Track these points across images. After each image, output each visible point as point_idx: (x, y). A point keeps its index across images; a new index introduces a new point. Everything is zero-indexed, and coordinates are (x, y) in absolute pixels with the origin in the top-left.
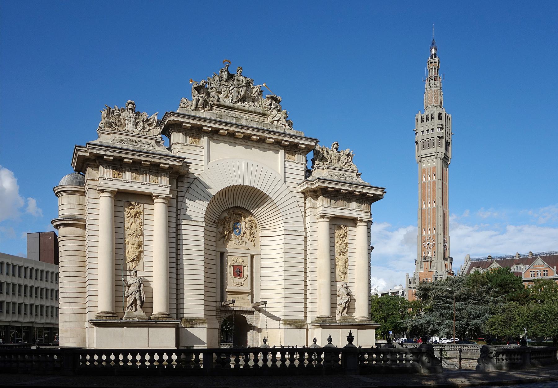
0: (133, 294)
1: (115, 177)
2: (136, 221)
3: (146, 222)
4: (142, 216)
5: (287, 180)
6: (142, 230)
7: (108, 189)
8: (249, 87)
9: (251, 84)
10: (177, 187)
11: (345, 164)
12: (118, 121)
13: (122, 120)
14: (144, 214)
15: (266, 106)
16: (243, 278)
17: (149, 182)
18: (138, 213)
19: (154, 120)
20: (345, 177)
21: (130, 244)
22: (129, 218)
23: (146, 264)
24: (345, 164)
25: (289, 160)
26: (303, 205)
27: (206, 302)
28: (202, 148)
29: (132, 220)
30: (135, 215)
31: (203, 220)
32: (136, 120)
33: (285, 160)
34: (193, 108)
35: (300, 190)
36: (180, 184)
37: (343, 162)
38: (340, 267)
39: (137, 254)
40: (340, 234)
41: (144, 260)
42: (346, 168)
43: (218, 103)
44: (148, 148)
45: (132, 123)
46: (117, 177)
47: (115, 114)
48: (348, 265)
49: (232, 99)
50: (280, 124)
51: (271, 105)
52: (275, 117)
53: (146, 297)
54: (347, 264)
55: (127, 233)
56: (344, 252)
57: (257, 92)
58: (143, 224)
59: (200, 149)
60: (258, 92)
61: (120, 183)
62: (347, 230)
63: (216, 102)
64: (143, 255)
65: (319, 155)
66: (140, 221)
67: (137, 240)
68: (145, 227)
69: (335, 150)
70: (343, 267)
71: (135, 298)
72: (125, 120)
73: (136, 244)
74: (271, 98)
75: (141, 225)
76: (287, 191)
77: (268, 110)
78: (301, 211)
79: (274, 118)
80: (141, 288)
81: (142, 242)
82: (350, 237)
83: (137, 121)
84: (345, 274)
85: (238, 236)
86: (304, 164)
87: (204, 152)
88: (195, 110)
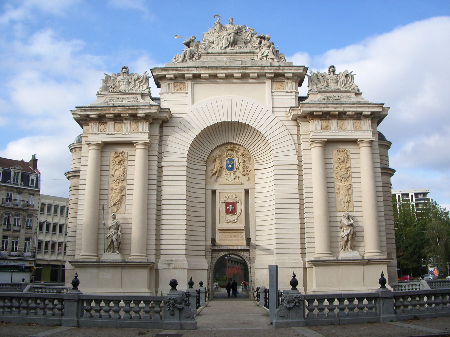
0: (110, 236)
1: (100, 132)
2: (120, 167)
3: (129, 168)
4: (125, 163)
5: (276, 110)
6: (125, 175)
7: (94, 143)
8: (242, 32)
9: (243, 30)
10: (161, 132)
11: (345, 85)
12: (113, 84)
13: (117, 83)
14: (127, 161)
15: (256, 45)
16: (236, 214)
17: (130, 131)
18: (122, 160)
19: (143, 78)
20: (339, 99)
21: (113, 189)
22: (114, 166)
23: (128, 207)
24: (345, 85)
25: (278, 90)
26: (296, 132)
27: (187, 241)
28: (186, 94)
29: (117, 167)
30: (119, 162)
31: (186, 159)
32: (128, 80)
33: (272, 91)
34: (181, 59)
35: (290, 118)
36: (164, 129)
37: (341, 84)
38: (341, 195)
39: (119, 197)
40: (339, 159)
41: (126, 203)
42: (345, 89)
43: (206, 52)
44: (132, 102)
45: (125, 84)
46: (102, 131)
47: (112, 79)
48: (353, 192)
49: (221, 46)
50: (269, 58)
51: (260, 43)
52: (263, 53)
53: (122, 239)
54: (350, 191)
55: (111, 179)
56: (346, 178)
57: (249, 35)
58: (127, 170)
59: (184, 95)
60: (250, 35)
61: (105, 136)
62: (348, 154)
63: (204, 52)
64: (125, 198)
65: (313, 81)
66: (124, 167)
67: (120, 185)
68: (128, 173)
69: (332, 73)
70: (345, 195)
71: (112, 240)
72: (119, 82)
73: (119, 189)
74: (259, 38)
75: (125, 171)
76: (276, 121)
77: (257, 49)
78: (293, 139)
79: (262, 54)
80: (119, 230)
81: (124, 186)
82: (353, 161)
83: (129, 81)
84: (349, 202)
85: (230, 172)
86: (294, 91)
87: (189, 96)
88: (182, 61)
